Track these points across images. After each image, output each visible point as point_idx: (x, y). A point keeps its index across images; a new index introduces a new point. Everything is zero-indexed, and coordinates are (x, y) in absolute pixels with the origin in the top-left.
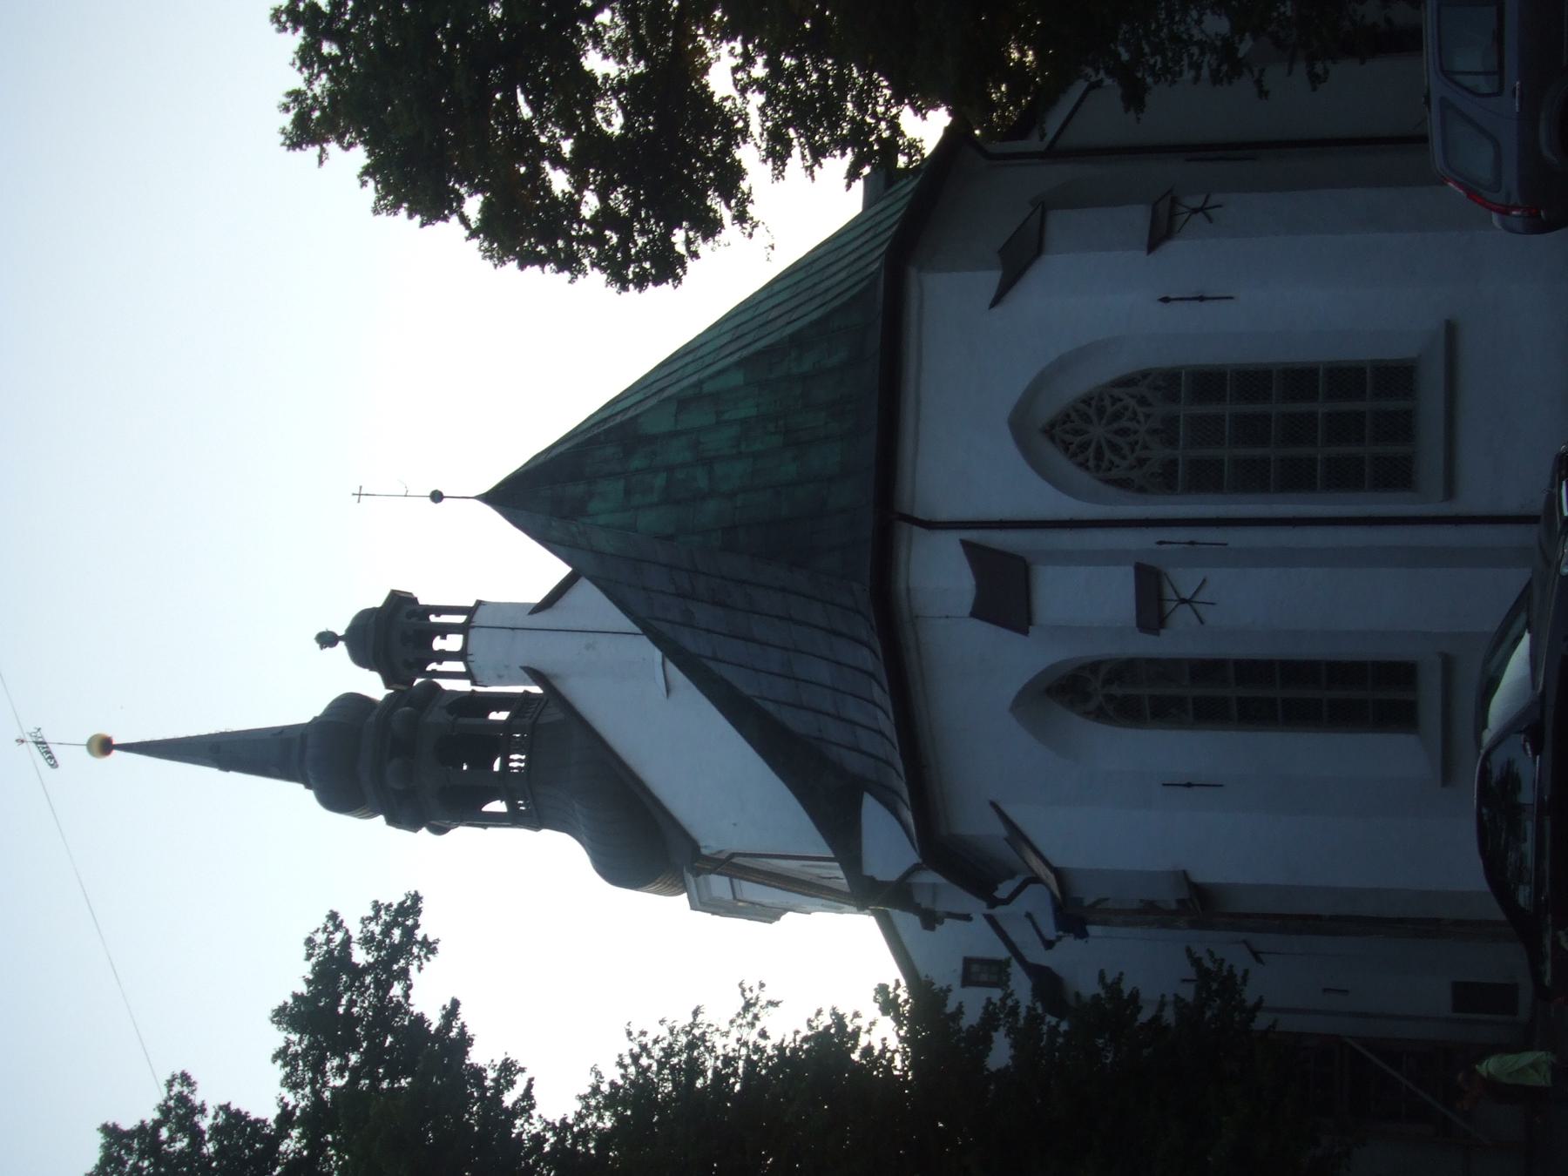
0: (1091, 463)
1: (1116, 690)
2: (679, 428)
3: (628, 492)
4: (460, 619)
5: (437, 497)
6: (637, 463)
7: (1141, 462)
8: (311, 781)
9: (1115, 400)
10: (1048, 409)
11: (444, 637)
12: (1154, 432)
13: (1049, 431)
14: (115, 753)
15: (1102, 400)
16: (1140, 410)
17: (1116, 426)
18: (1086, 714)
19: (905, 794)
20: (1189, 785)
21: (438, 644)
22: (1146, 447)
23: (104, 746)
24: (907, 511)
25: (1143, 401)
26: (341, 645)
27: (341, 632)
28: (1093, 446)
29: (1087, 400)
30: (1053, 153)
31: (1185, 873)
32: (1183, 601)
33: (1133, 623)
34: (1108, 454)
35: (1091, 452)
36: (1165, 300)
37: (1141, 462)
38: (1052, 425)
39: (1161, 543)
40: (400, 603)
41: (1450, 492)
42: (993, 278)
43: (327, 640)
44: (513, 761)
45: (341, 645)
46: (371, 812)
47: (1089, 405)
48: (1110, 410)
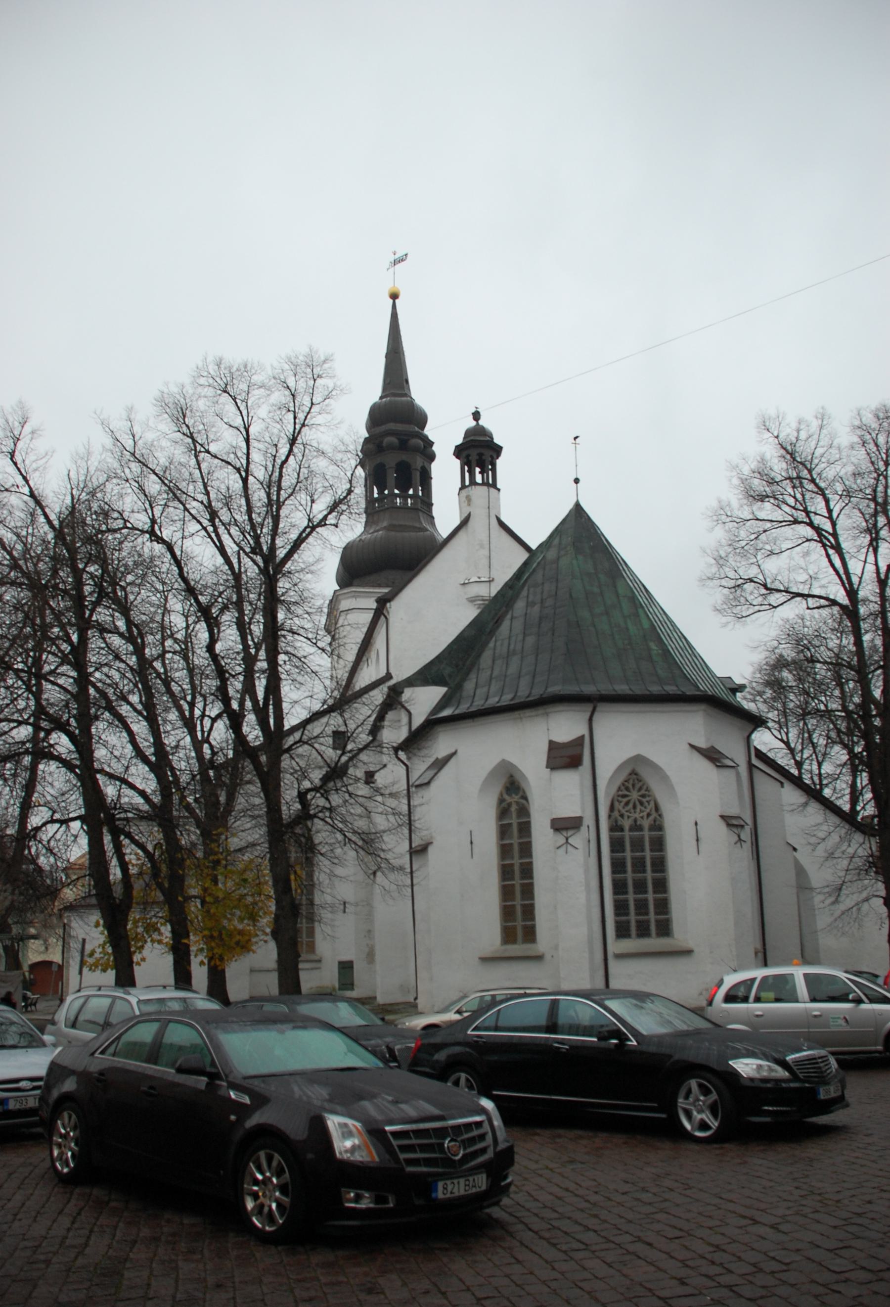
0: (620, 793)
1: (514, 808)
4: (491, 482)
5: (577, 481)
6: (602, 577)
7: (622, 816)
8: (384, 400)
9: (648, 802)
10: (644, 772)
12: (635, 820)
13: (634, 773)
14: (391, 301)
15: (649, 796)
16: (645, 814)
18: (501, 794)
19: (457, 712)
20: (471, 843)
21: (478, 470)
22: (629, 817)
23: (394, 296)
24: (598, 709)
25: (649, 815)
26: (474, 423)
27: (481, 422)
28: (627, 793)
29: (647, 790)
30: (751, 766)
31: (431, 843)
32: (567, 839)
33: (555, 816)
34: (625, 800)
36: (696, 824)
38: (636, 774)
40: (497, 450)
41: (619, 956)
42: (702, 744)
43: (476, 416)
45: (474, 423)
46: (369, 428)
48: (644, 800)
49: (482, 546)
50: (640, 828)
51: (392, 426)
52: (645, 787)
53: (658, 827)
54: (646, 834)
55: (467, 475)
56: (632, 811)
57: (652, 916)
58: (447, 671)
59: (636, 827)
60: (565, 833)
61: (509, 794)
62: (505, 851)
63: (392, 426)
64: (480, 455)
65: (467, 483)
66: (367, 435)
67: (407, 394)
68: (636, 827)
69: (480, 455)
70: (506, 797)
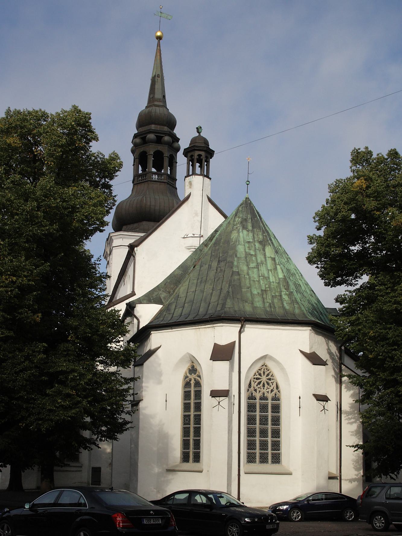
0: (255, 377)
1: (193, 382)
2: (267, 258)
3: (249, 242)
4: (205, 174)
6: (257, 245)
10: (271, 365)
11: (199, 167)
12: (264, 394)
16: (270, 390)
17: (265, 383)
20: (166, 401)
25: (272, 391)
26: (198, 134)
27: (201, 134)
31: (143, 400)
32: (219, 403)
35: (259, 377)
36: (300, 398)
37: (255, 390)
39: (234, 396)
40: (210, 153)
42: (308, 351)
44: (155, 176)
47: (271, 376)
48: (270, 382)
49: (196, 214)
50: (267, 399)
51: (153, 127)
52: (271, 374)
53: (276, 398)
54: (270, 402)
55: (191, 167)
56: (262, 388)
57: (270, 451)
58: (163, 295)
59: (264, 398)
60: (218, 398)
61: (191, 374)
62: (186, 407)
63: (153, 127)
64: (200, 156)
65: (191, 173)
66: (136, 132)
67: (165, 106)
68: (264, 398)
69: (200, 156)
70: (188, 375)
